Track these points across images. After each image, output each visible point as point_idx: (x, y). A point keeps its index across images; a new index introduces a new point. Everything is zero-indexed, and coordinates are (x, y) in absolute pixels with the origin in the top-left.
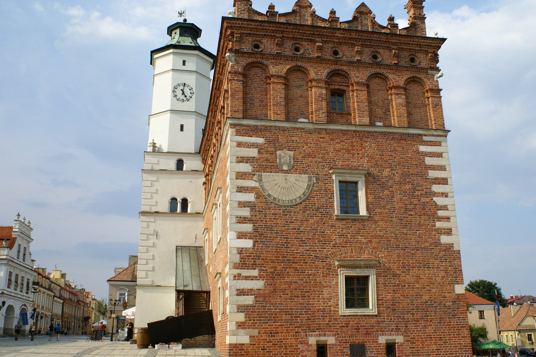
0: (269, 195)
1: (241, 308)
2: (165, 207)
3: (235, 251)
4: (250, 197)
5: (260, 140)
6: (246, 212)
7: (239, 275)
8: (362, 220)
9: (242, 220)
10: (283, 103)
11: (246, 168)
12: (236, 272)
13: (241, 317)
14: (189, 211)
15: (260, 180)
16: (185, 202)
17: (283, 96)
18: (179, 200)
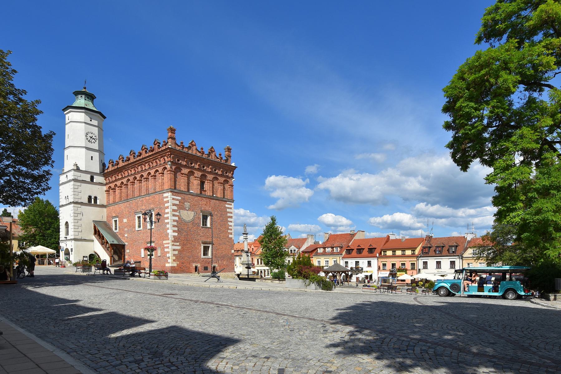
0: (182, 218)
1: (174, 255)
2: (86, 201)
3: (172, 236)
4: (177, 218)
5: (180, 198)
6: (175, 223)
7: (174, 244)
8: (208, 228)
9: (174, 226)
10: (187, 185)
11: (175, 208)
12: (173, 243)
13: (174, 258)
14: (98, 203)
15: (180, 213)
16: (96, 198)
17: (187, 182)
18: (93, 197)
